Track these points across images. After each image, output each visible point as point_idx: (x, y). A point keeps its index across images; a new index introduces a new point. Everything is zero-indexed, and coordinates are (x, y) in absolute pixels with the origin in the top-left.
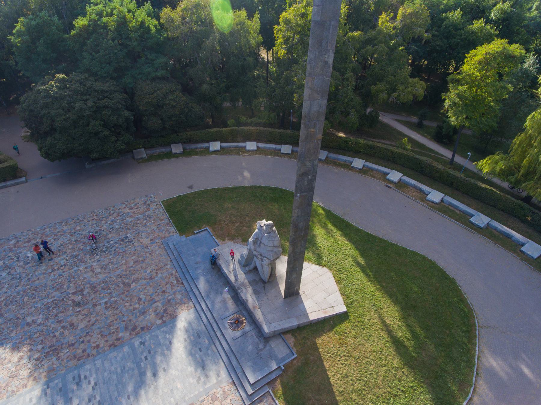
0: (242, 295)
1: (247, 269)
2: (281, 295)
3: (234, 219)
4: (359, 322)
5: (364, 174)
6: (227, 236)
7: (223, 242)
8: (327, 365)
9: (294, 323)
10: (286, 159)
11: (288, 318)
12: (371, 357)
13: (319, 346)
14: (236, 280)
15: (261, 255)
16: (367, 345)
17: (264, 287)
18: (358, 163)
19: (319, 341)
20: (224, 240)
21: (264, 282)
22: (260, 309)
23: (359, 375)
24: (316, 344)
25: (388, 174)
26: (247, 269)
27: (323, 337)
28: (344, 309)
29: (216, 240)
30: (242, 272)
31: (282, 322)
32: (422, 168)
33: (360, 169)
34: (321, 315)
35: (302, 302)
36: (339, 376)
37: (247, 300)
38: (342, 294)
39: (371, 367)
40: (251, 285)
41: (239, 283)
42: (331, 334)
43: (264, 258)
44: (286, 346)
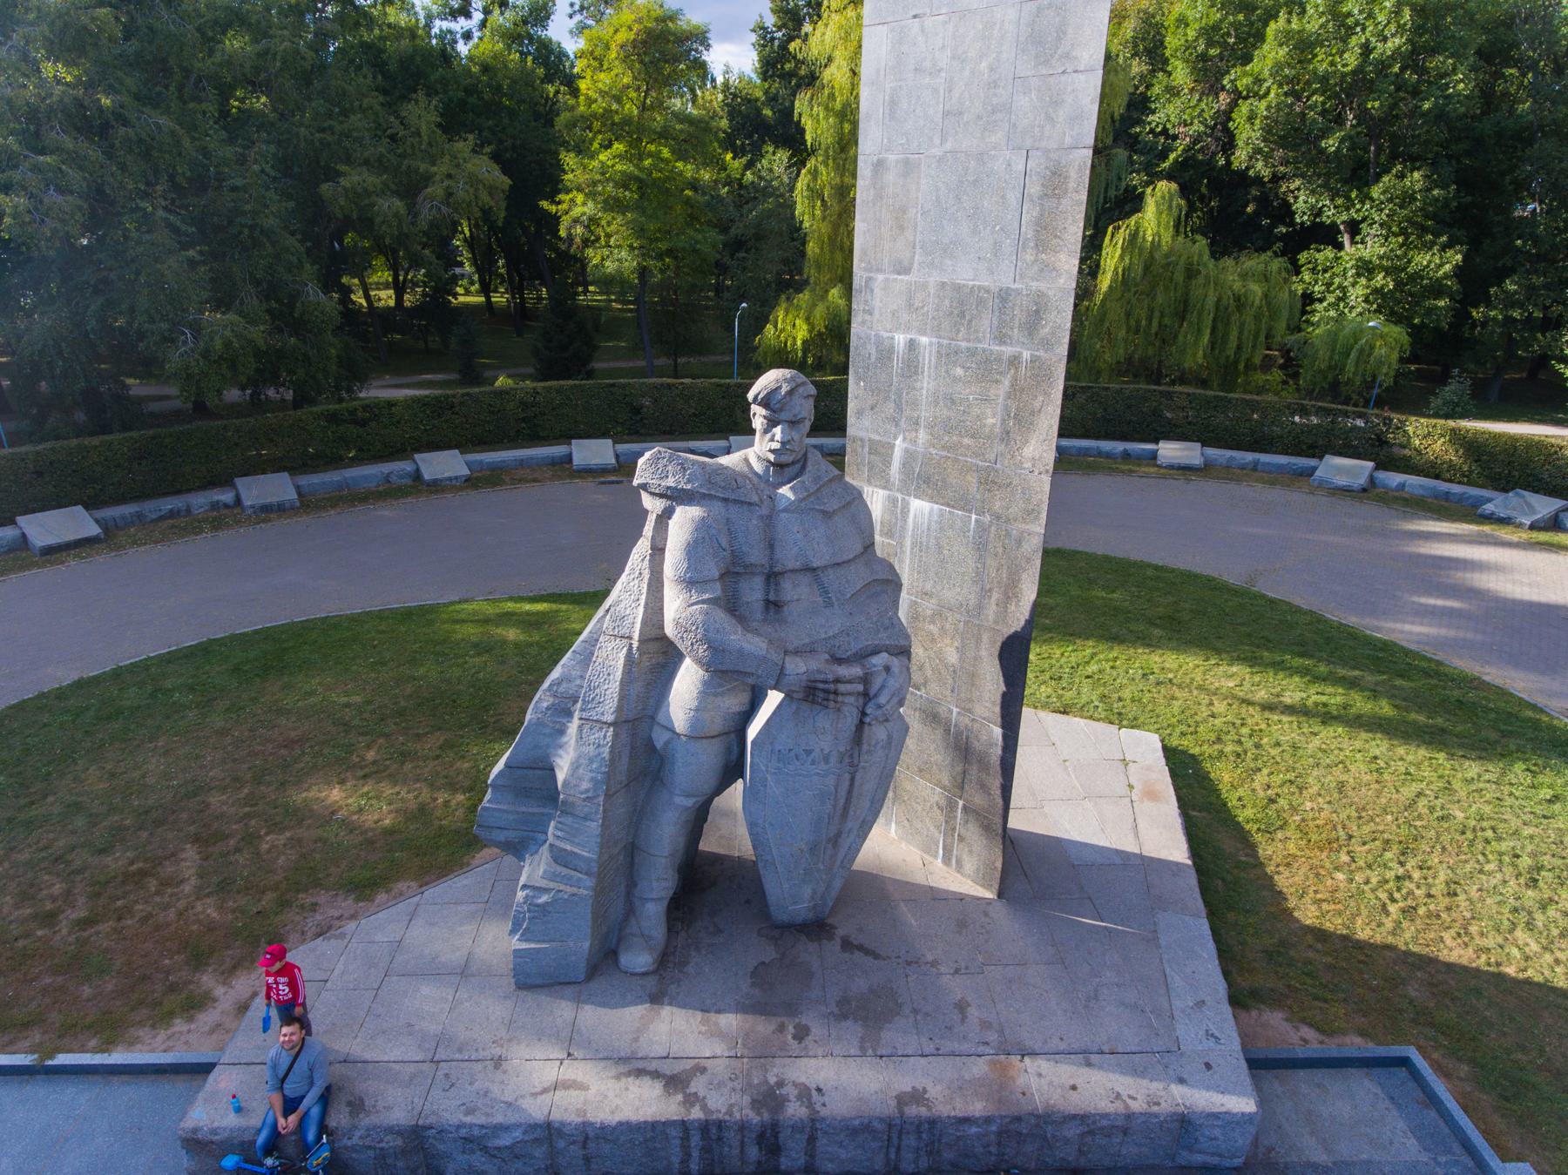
0: (836, 1107)
1: (638, 959)
2: (961, 898)
3: (116, 861)
4: (1219, 740)
5: (495, 484)
6: (199, 960)
7: (207, 1018)
8: (1454, 952)
9: (1191, 931)
10: (100, 559)
11: (1152, 940)
12: (1409, 791)
13: (1334, 924)
14: (674, 1083)
15: (840, 661)
16: (1344, 777)
17: (847, 945)
18: (444, 464)
19: (1308, 914)
20: (195, 1004)
21: (817, 928)
22: (1033, 1054)
23: (1508, 871)
24: (1320, 935)
25: (569, 458)
26: (638, 959)
27: (1282, 881)
28: (1146, 747)
29: (117, 1057)
30: (637, 1012)
31: (1177, 981)
32: (637, 411)
33: (468, 479)
34: (1168, 809)
35: (1058, 840)
36: (1520, 935)
37: (918, 1096)
38: (1064, 713)
39: (1460, 815)
40: (791, 1009)
41: (720, 1068)
42: (1266, 850)
43: (881, 659)
44: (1320, 1075)
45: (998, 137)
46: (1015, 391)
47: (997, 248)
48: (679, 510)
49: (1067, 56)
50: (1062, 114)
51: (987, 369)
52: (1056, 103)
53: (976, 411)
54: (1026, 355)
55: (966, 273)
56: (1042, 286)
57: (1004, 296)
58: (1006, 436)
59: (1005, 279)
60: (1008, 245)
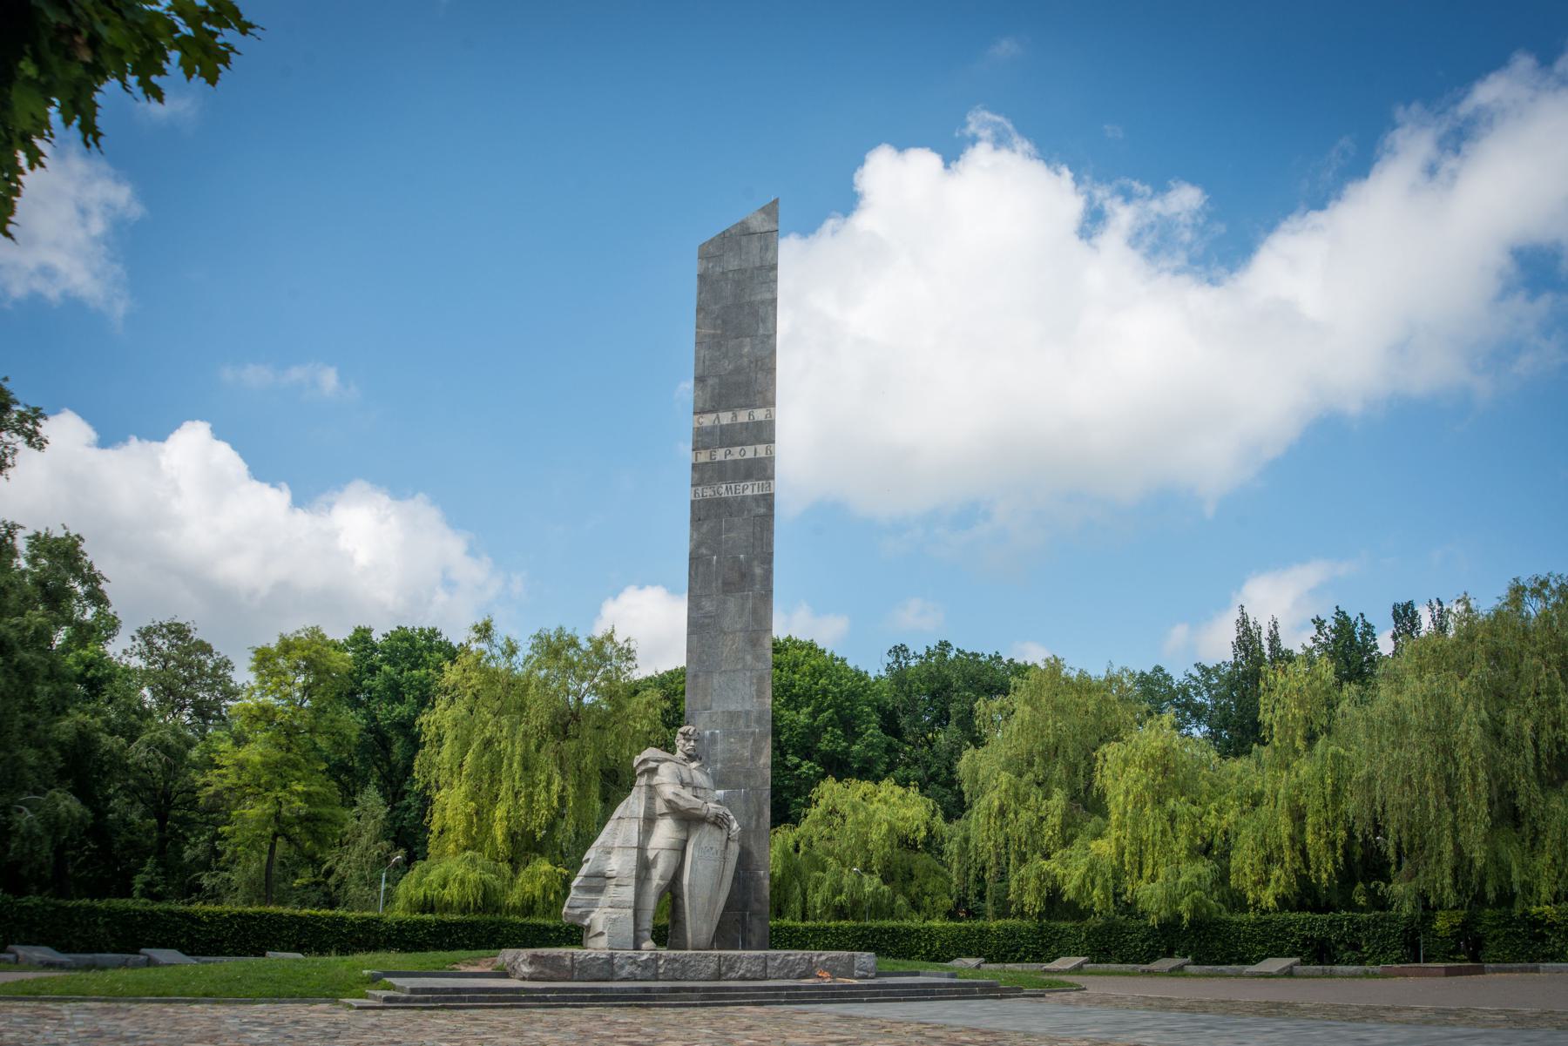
51: (743, 737)
55: (732, 708)
57: (748, 713)
59: (748, 707)
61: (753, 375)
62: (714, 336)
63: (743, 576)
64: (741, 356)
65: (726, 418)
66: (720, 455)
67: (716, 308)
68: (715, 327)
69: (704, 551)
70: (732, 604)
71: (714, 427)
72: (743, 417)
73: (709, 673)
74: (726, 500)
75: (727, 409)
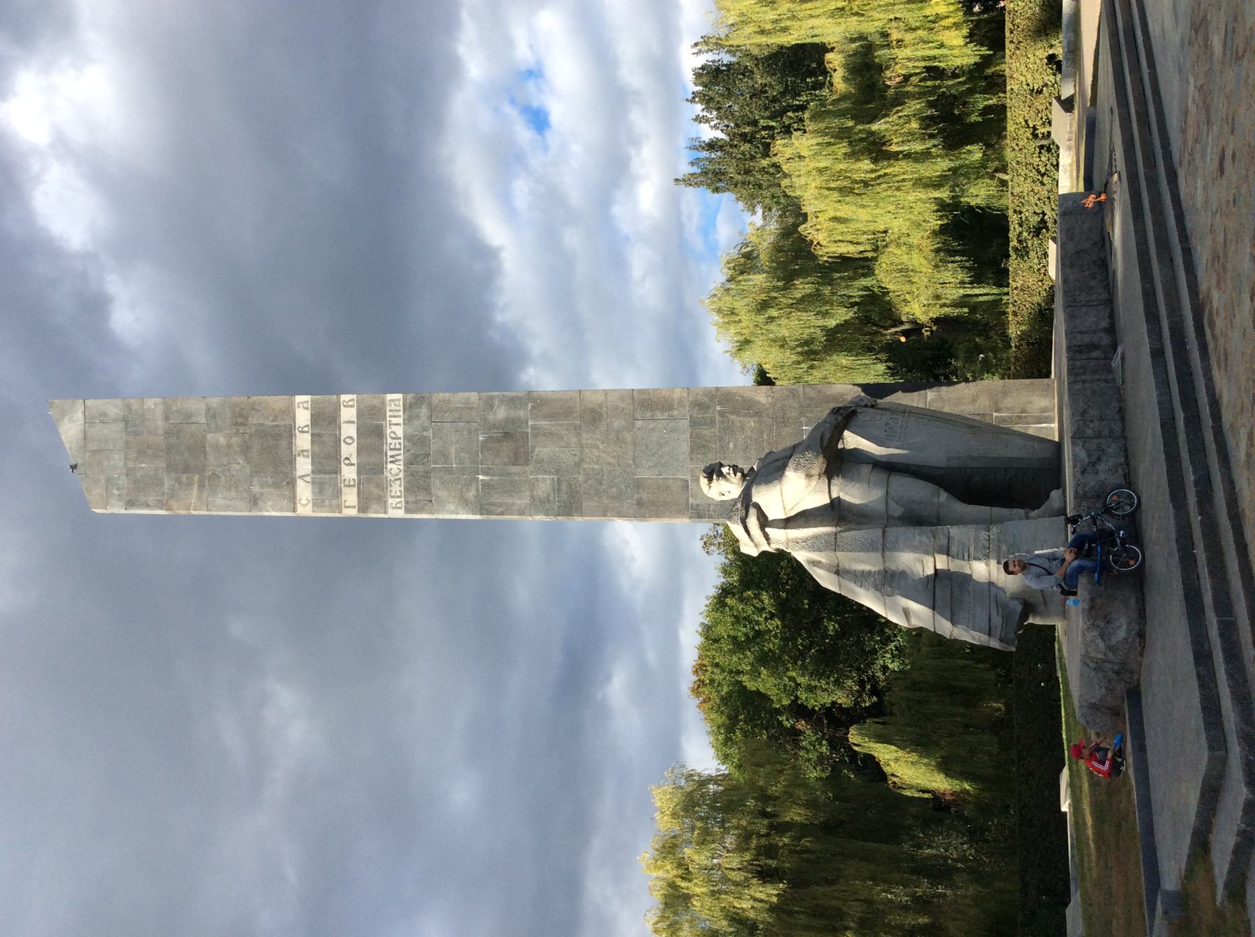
45: (628, 437)
46: (735, 411)
47: (673, 430)
48: (754, 499)
49: (600, 407)
50: (621, 405)
51: (728, 429)
52: (616, 408)
53: (749, 433)
54: (718, 408)
55: (685, 447)
56: (687, 404)
57: (694, 423)
58: (758, 414)
59: (686, 423)
60: (672, 424)
61: (253, 430)
62: (201, 486)
63: (507, 435)
64: (229, 446)
65: (304, 466)
66: (349, 473)
67: (168, 483)
68: (190, 485)
69: (471, 494)
70: (544, 450)
71: (313, 483)
72: (303, 441)
73: (639, 485)
74: (409, 463)
75: (292, 462)
